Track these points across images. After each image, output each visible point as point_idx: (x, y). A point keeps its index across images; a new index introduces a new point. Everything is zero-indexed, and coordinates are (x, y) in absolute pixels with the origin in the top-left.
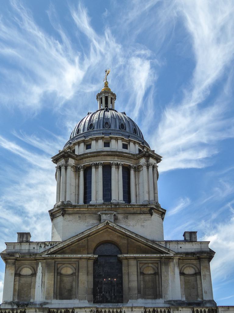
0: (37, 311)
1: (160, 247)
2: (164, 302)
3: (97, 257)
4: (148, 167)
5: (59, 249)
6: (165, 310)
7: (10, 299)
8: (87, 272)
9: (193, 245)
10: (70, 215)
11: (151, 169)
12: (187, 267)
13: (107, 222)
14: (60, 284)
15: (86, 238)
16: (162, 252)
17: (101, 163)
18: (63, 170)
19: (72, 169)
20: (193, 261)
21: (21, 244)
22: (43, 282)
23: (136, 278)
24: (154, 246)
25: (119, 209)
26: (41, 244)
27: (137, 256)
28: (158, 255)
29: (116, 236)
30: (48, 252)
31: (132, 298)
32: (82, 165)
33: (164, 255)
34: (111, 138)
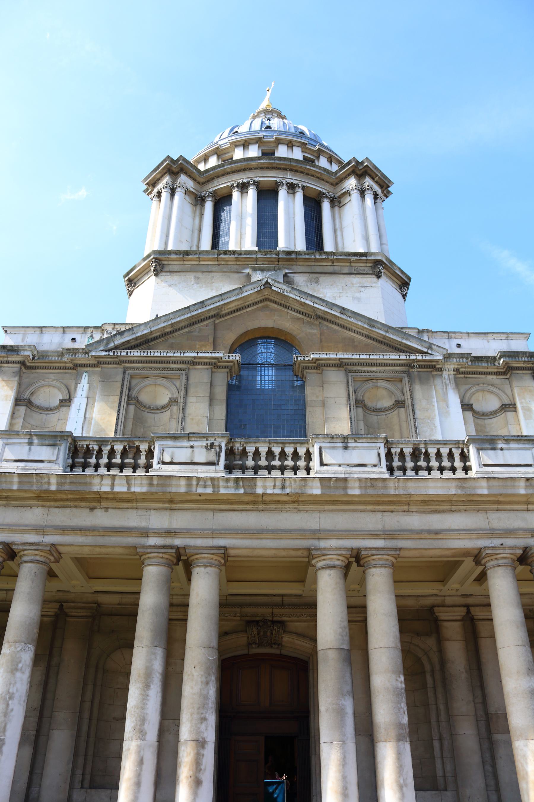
0: (36, 441)
1: (406, 339)
3: (238, 358)
4: (362, 193)
5: (136, 339)
6: (451, 449)
8: (208, 395)
9: (488, 342)
10: (175, 274)
12: (477, 391)
13: (267, 282)
14: (134, 425)
15: (209, 318)
17: (254, 182)
19: (187, 197)
20: (493, 378)
21: (41, 330)
22: (87, 420)
24: (391, 336)
25: (298, 263)
26: (92, 332)
27: (346, 356)
28: (403, 357)
29: (289, 317)
30: (108, 344)
32: (211, 190)
33: (419, 357)
34: (278, 142)
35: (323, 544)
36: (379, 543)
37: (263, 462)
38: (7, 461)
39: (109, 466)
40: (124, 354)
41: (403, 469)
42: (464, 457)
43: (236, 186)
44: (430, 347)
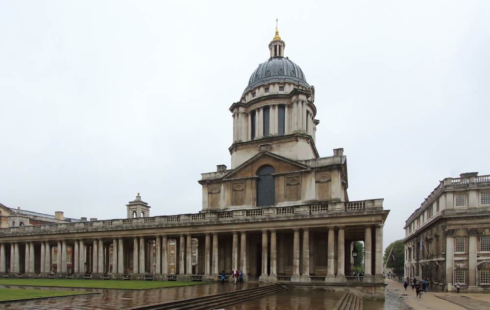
11: (300, 104)
18: (236, 117)
19: (243, 115)
23: (283, 188)
31: (280, 201)
35: (263, 229)
36: (273, 229)
42: (293, 209)
44: (307, 166)
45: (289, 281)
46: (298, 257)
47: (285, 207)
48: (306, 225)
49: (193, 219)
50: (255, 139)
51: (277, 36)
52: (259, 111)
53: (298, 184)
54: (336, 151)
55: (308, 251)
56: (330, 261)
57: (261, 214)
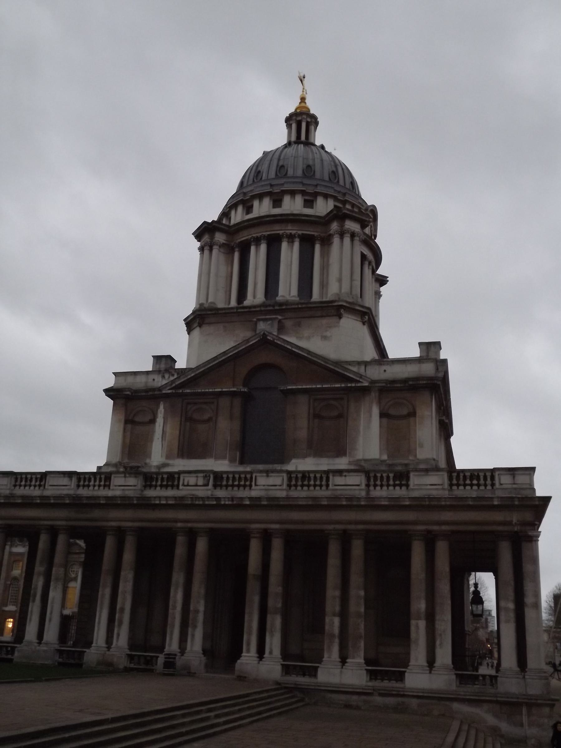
0: (127, 475)
2: (347, 462)
4: (342, 235)
7: (116, 459)
13: (264, 334)
16: (351, 380)
17: (264, 235)
19: (222, 250)
27: (308, 387)
30: (171, 385)
34: (284, 192)
36: (277, 526)
37: (230, 482)
38: (116, 486)
39: (161, 486)
40: (181, 391)
41: (296, 486)
43: (253, 240)
44: (361, 376)
45: (313, 680)
46: (338, 609)
47: (309, 472)
48: (357, 523)
49: (78, 486)
50: (246, 303)
51: (303, 104)
52: (258, 245)
53: (340, 416)
54: (424, 347)
55: (362, 593)
56: (417, 626)
57: (251, 486)
